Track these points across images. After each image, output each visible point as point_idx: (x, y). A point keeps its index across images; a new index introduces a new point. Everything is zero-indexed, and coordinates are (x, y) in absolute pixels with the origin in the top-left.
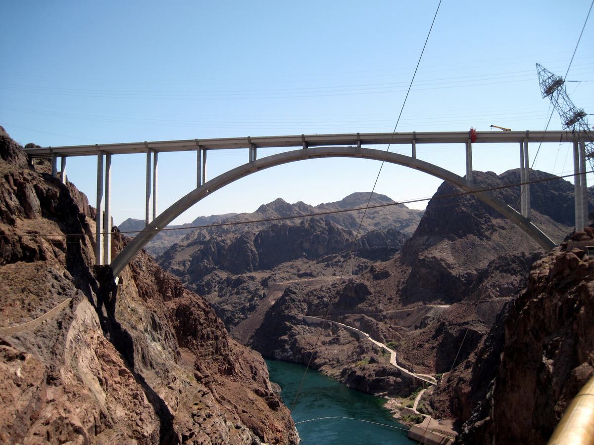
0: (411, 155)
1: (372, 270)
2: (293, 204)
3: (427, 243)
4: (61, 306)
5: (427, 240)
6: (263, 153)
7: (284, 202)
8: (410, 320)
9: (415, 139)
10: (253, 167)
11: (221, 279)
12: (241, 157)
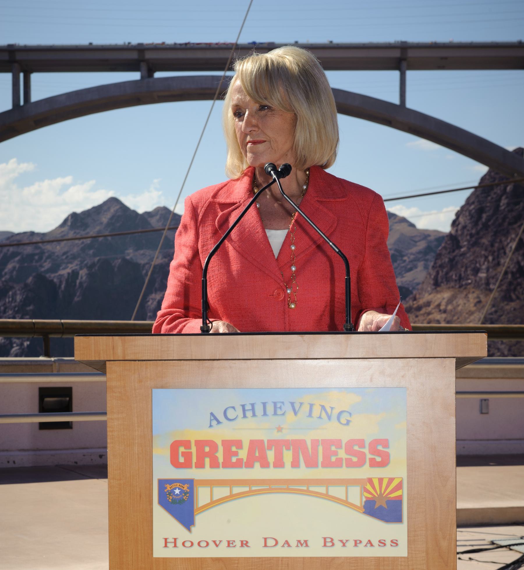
0: (396, 100)
2: (147, 214)
3: (450, 307)
5: (450, 301)
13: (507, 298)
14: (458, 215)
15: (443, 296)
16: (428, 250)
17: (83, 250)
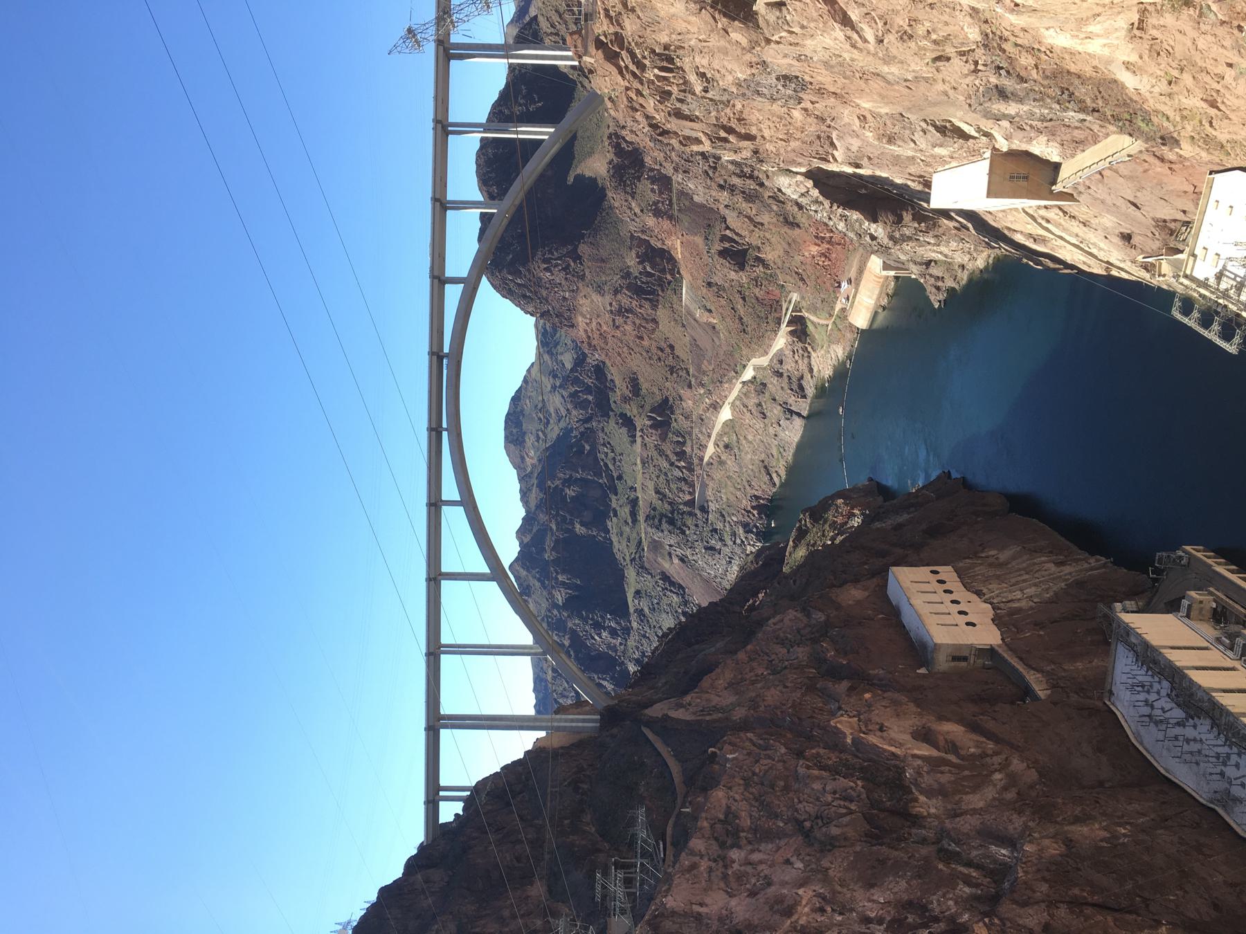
1: (625, 400)
4: (650, 735)
5: (584, 317)
6: (450, 490)
7: (517, 560)
8: (704, 342)
9: (439, 280)
10: (468, 502)
11: (637, 648)
12: (454, 520)
13: (583, 277)
14: (527, 312)
15: (580, 320)
16: (550, 353)
17: (545, 588)
